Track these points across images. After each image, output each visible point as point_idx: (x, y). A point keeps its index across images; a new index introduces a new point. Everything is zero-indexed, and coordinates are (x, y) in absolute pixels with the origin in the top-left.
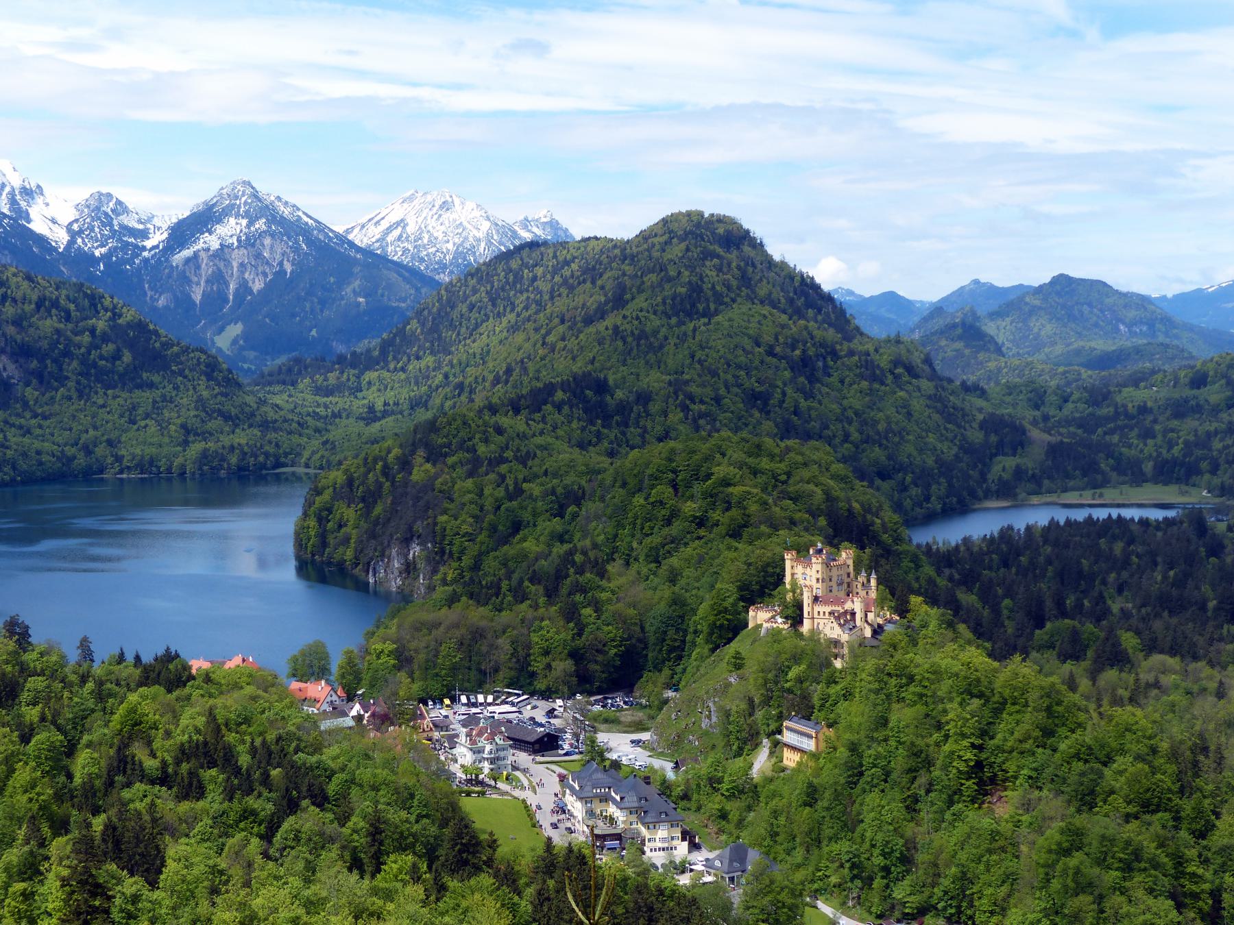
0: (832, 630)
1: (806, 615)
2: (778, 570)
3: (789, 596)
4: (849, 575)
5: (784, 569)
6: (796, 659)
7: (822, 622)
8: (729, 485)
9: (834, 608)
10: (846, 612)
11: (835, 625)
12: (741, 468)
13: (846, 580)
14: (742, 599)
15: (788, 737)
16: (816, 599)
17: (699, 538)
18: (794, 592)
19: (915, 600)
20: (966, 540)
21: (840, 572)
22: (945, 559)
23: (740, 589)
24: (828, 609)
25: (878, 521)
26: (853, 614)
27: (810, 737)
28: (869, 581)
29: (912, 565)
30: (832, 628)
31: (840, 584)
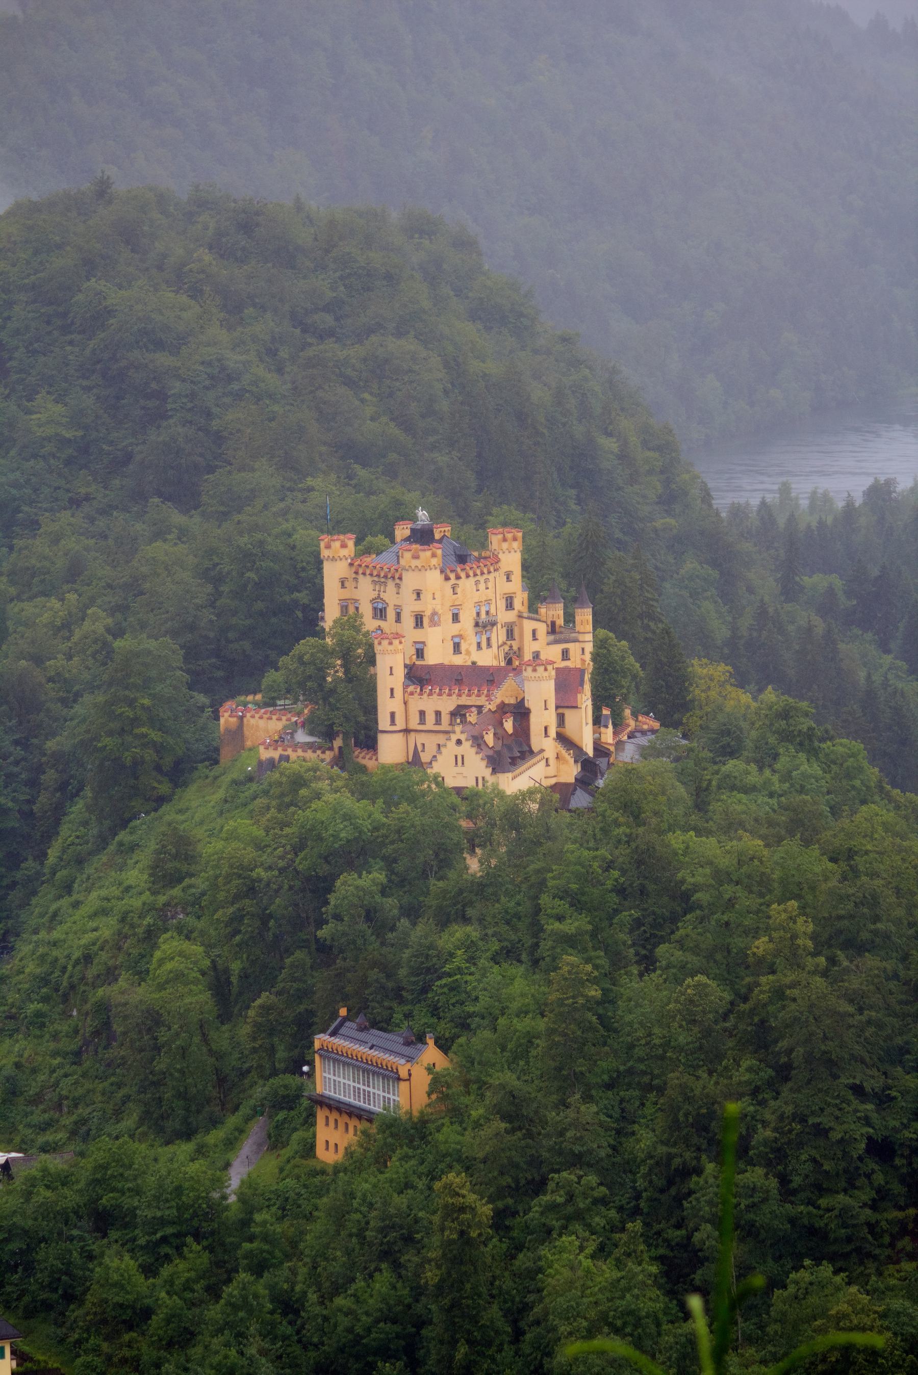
0: (460, 767)
1: (384, 722)
2: (303, 597)
3: (335, 672)
4: (510, 606)
5: (318, 594)
6: (356, 854)
7: (430, 742)
8: (159, 345)
9: (464, 700)
10: (503, 709)
11: (467, 748)
12: (195, 293)
13: (505, 617)
14: (197, 681)
15: (329, 1081)
16: (419, 676)
17: (75, 503)
18: (346, 655)
19: (708, 676)
20: (880, 493)
21: (484, 594)
22: (799, 546)
23: (191, 653)
24: (447, 704)
25: (610, 444)
26: (521, 713)
27: (392, 1077)
28: (570, 618)
29: (715, 574)
30: (459, 760)
31: (483, 625)
